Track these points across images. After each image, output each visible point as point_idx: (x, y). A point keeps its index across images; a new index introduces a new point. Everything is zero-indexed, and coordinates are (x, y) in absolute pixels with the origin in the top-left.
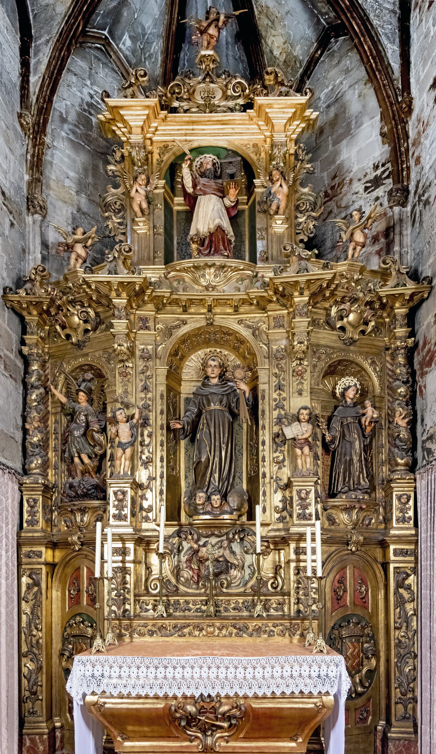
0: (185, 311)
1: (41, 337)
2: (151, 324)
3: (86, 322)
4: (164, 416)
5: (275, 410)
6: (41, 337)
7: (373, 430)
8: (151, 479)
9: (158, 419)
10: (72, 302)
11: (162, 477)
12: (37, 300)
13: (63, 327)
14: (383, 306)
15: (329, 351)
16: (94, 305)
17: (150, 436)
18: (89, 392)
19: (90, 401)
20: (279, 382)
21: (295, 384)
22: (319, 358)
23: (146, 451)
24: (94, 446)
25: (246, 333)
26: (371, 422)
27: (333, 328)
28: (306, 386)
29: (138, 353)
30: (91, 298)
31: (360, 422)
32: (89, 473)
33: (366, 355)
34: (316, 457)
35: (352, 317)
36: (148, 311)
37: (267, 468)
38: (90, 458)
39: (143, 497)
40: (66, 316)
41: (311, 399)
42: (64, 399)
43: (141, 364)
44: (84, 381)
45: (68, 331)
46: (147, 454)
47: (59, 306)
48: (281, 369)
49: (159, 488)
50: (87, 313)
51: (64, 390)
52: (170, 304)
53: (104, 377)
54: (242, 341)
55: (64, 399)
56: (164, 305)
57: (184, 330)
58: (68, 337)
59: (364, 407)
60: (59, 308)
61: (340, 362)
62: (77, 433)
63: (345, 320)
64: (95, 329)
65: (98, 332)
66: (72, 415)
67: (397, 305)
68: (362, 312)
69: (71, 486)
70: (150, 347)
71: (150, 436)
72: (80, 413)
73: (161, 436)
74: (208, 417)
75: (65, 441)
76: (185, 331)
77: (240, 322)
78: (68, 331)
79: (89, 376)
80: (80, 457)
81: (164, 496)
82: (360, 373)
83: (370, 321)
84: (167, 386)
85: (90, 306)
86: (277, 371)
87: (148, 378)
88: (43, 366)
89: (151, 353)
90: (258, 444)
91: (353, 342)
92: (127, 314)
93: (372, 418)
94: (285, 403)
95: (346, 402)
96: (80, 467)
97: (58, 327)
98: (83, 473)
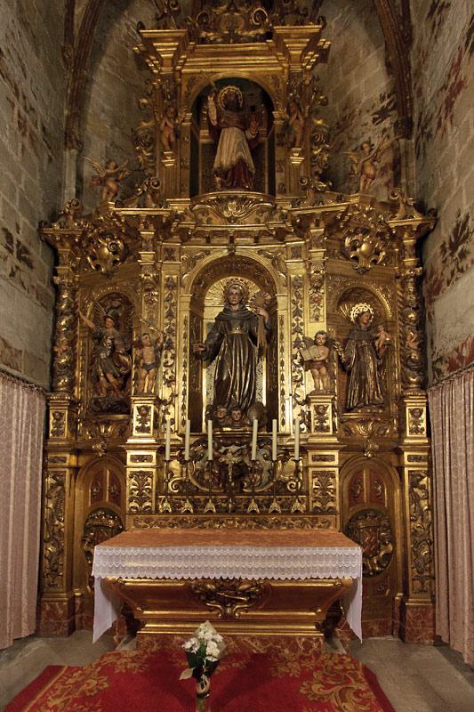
0: (208, 242)
1: (72, 268)
2: (176, 255)
3: (115, 253)
4: (188, 340)
5: (293, 334)
6: (72, 268)
7: (386, 352)
8: (174, 395)
9: (181, 342)
10: (103, 236)
11: (184, 394)
12: (70, 233)
13: (93, 258)
14: (393, 237)
15: (344, 280)
16: (123, 237)
17: (173, 357)
18: (116, 318)
19: (117, 326)
20: (297, 308)
21: (312, 310)
22: (334, 286)
23: (169, 371)
24: (120, 367)
25: (265, 262)
26: (384, 345)
27: (347, 258)
28: (323, 312)
29: (163, 282)
30: (121, 231)
31: (373, 344)
32: (114, 390)
33: (379, 284)
34: (333, 377)
35: (364, 247)
36: (174, 243)
37: (286, 386)
38: (115, 377)
39: (166, 412)
40: (96, 248)
41: (328, 324)
42: (91, 325)
43: (166, 293)
44: (112, 308)
45: (98, 262)
46: (170, 374)
47: (91, 238)
48: (299, 297)
49: (181, 404)
50: (117, 245)
51: (92, 316)
52: (194, 235)
53: (131, 304)
54: (262, 270)
55: (91, 325)
56: (189, 237)
57: (208, 259)
58: (98, 267)
59: (378, 331)
60: (90, 240)
61: (354, 290)
62: (103, 355)
63: (358, 250)
64: (123, 260)
65: (126, 262)
66: (99, 339)
67: (406, 236)
68: (374, 243)
69: (96, 402)
70: (174, 277)
71: (173, 357)
72: (107, 338)
73: (183, 358)
74: (230, 341)
75: (92, 363)
76: (208, 261)
77: (260, 252)
78: (98, 262)
79: (116, 303)
80: (105, 376)
81: (186, 411)
82: (372, 300)
83: (382, 251)
84: (190, 311)
85: (119, 238)
86: (295, 298)
87: (173, 305)
88: (73, 293)
89: (175, 281)
90: (277, 365)
91: (366, 271)
92: (154, 246)
93: (386, 341)
94: (302, 327)
95: (360, 327)
96: (105, 385)
97: (89, 258)
98: (108, 390)
